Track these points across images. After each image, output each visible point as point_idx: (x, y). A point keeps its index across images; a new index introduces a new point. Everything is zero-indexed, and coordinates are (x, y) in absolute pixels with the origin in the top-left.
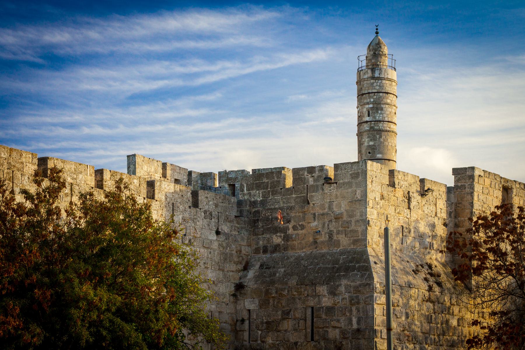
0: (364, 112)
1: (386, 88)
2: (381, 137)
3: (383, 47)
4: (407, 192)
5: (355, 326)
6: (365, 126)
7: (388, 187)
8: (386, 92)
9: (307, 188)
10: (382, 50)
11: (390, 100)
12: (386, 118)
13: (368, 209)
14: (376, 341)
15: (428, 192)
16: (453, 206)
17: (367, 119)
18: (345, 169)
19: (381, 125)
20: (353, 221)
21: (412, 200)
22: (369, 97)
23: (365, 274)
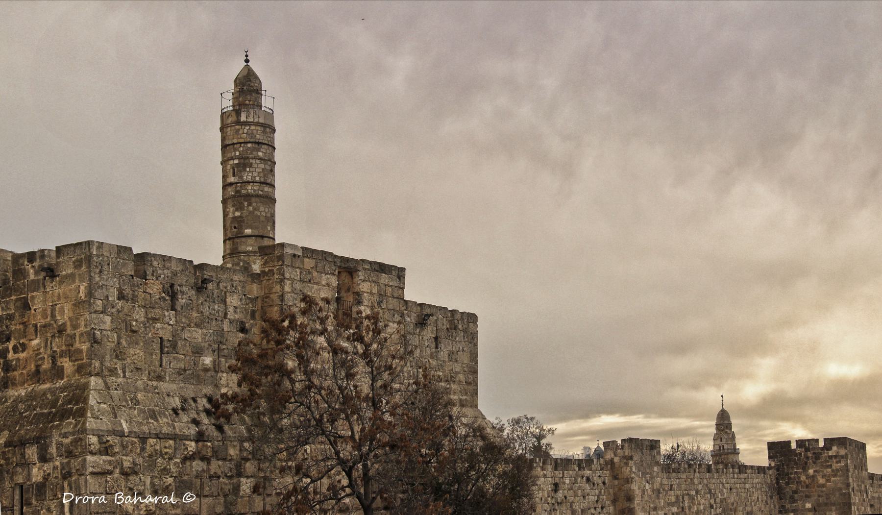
1: (255, 136)
2: (250, 204)
6: (229, 190)
7: (133, 278)
8: (257, 141)
9: (28, 285)
10: (252, 84)
11: (262, 152)
12: (256, 177)
15: (207, 284)
17: (232, 179)
19: (249, 187)
22: (234, 149)
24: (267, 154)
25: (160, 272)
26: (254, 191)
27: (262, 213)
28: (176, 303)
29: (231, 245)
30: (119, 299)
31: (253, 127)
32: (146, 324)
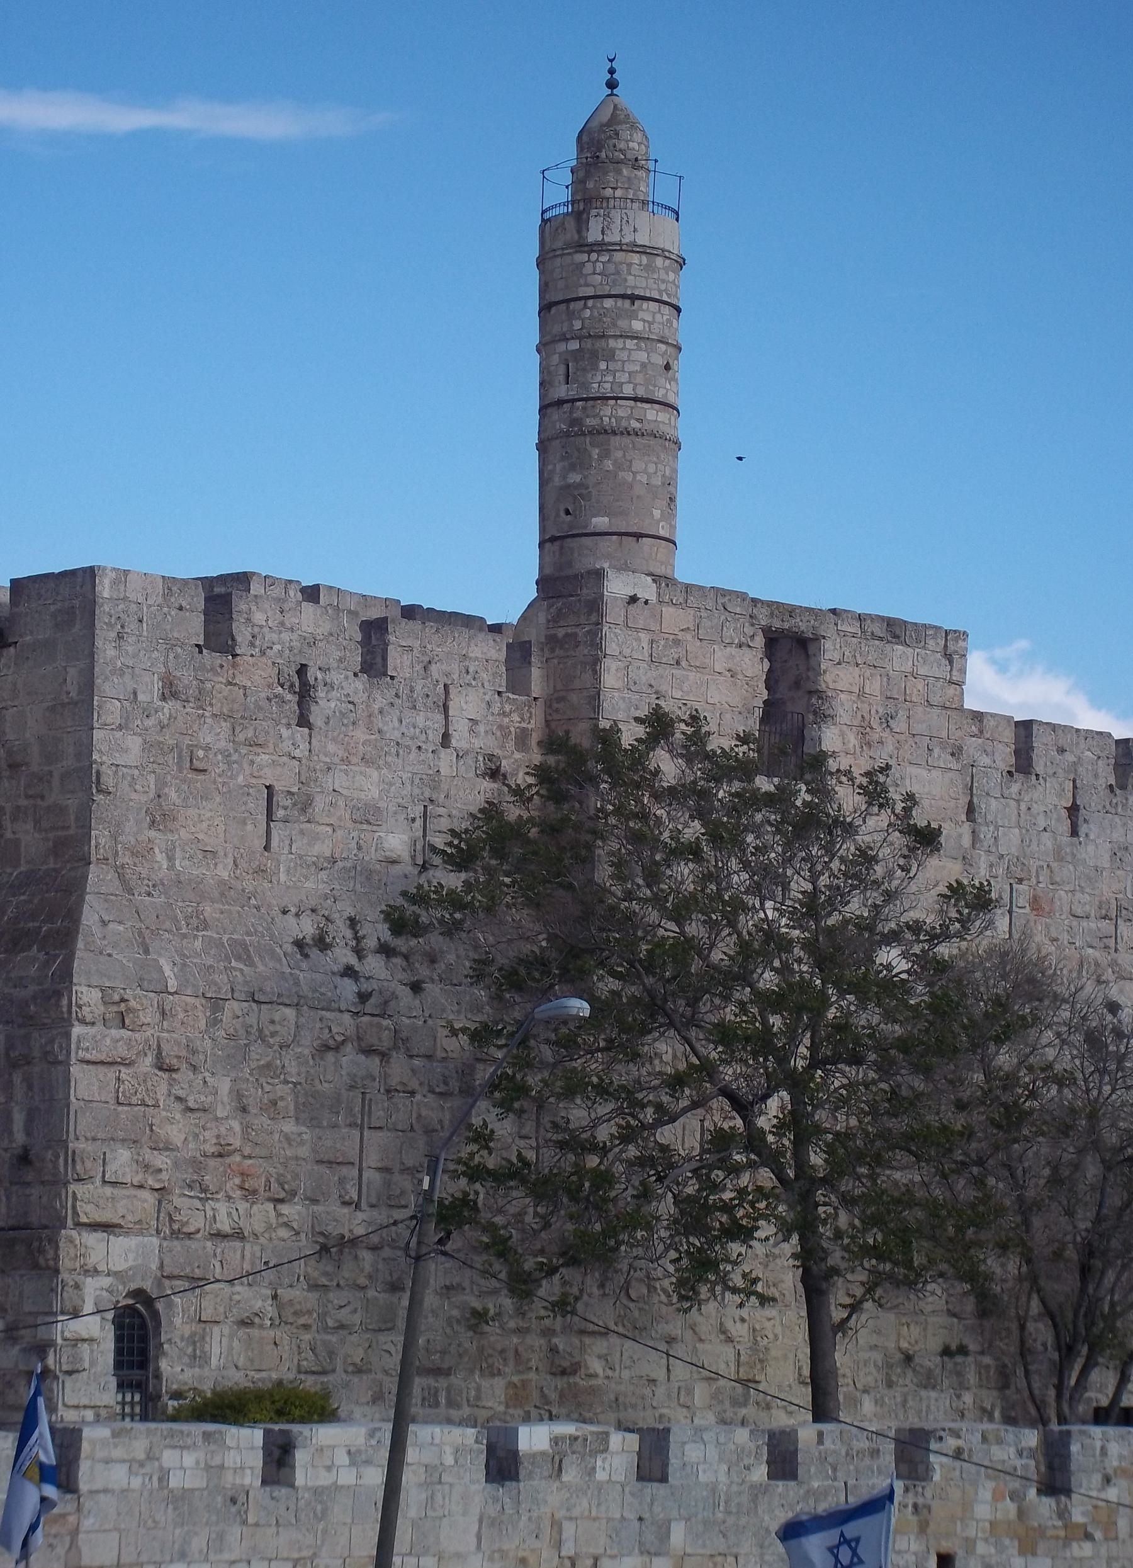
0: (552, 368)
1: (626, 280)
2: (606, 454)
3: (625, 134)
4: (294, 668)
5: (20, 1138)
6: (555, 417)
7: (201, 652)
10: (622, 145)
11: (644, 321)
13: (97, 735)
14: (74, 1193)
16: (538, 711)
17: (561, 391)
18: (40, 596)
19: (607, 411)
20: (56, 775)
21: (321, 693)
23: (57, 956)
24: (656, 325)
25: (270, 636)
26: (619, 419)
27: (638, 478)
28: (312, 708)
29: (557, 554)
30: (164, 698)
31: (619, 256)
32: (229, 755)
